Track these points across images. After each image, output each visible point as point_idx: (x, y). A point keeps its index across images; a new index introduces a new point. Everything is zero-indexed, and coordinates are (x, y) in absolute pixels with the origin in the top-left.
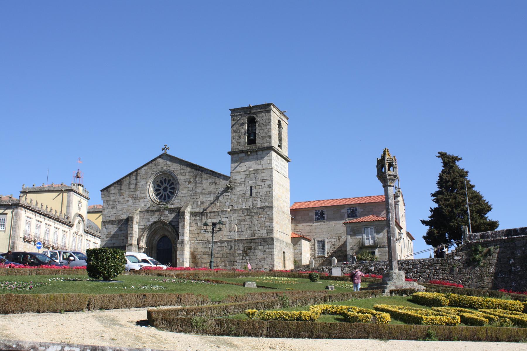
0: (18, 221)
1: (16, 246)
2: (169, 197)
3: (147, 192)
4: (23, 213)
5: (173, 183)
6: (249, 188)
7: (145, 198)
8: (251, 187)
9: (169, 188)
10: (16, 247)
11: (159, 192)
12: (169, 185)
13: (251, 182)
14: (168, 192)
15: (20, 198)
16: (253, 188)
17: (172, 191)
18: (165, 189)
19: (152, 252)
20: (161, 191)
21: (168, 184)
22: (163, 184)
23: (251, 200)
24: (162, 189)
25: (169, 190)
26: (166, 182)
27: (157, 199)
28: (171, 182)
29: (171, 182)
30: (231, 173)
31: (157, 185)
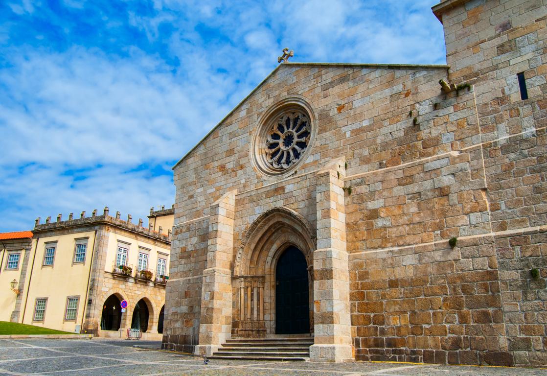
0: (101, 248)
1: (96, 285)
2: (297, 155)
3: (251, 154)
4: (112, 238)
5: (303, 124)
6: (514, 80)
7: (246, 165)
8: (521, 77)
9: (295, 135)
10: (96, 287)
11: (273, 150)
12: (295, 130)
13: (519, 63)
14: (294, 145)
15: (105, 213)
16: (526, 76)
17: (303, 140)
18: (288, 140)
19: (247, 290)
20: (282, 147)
21: (293, 129)
22: (282, 131)
23: (525, 110)
24: (281, 141)
25: (296, 140)
26: (290, 126)
27: (272, 165)
28: (299, 122)
29: (299, 122)
30: (447, 56)
31: (272, 135)
